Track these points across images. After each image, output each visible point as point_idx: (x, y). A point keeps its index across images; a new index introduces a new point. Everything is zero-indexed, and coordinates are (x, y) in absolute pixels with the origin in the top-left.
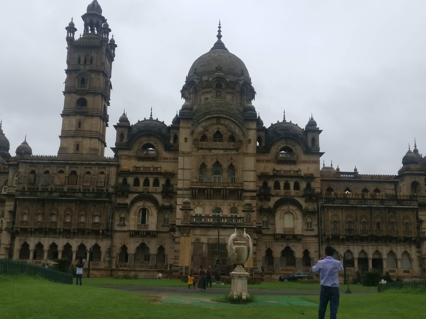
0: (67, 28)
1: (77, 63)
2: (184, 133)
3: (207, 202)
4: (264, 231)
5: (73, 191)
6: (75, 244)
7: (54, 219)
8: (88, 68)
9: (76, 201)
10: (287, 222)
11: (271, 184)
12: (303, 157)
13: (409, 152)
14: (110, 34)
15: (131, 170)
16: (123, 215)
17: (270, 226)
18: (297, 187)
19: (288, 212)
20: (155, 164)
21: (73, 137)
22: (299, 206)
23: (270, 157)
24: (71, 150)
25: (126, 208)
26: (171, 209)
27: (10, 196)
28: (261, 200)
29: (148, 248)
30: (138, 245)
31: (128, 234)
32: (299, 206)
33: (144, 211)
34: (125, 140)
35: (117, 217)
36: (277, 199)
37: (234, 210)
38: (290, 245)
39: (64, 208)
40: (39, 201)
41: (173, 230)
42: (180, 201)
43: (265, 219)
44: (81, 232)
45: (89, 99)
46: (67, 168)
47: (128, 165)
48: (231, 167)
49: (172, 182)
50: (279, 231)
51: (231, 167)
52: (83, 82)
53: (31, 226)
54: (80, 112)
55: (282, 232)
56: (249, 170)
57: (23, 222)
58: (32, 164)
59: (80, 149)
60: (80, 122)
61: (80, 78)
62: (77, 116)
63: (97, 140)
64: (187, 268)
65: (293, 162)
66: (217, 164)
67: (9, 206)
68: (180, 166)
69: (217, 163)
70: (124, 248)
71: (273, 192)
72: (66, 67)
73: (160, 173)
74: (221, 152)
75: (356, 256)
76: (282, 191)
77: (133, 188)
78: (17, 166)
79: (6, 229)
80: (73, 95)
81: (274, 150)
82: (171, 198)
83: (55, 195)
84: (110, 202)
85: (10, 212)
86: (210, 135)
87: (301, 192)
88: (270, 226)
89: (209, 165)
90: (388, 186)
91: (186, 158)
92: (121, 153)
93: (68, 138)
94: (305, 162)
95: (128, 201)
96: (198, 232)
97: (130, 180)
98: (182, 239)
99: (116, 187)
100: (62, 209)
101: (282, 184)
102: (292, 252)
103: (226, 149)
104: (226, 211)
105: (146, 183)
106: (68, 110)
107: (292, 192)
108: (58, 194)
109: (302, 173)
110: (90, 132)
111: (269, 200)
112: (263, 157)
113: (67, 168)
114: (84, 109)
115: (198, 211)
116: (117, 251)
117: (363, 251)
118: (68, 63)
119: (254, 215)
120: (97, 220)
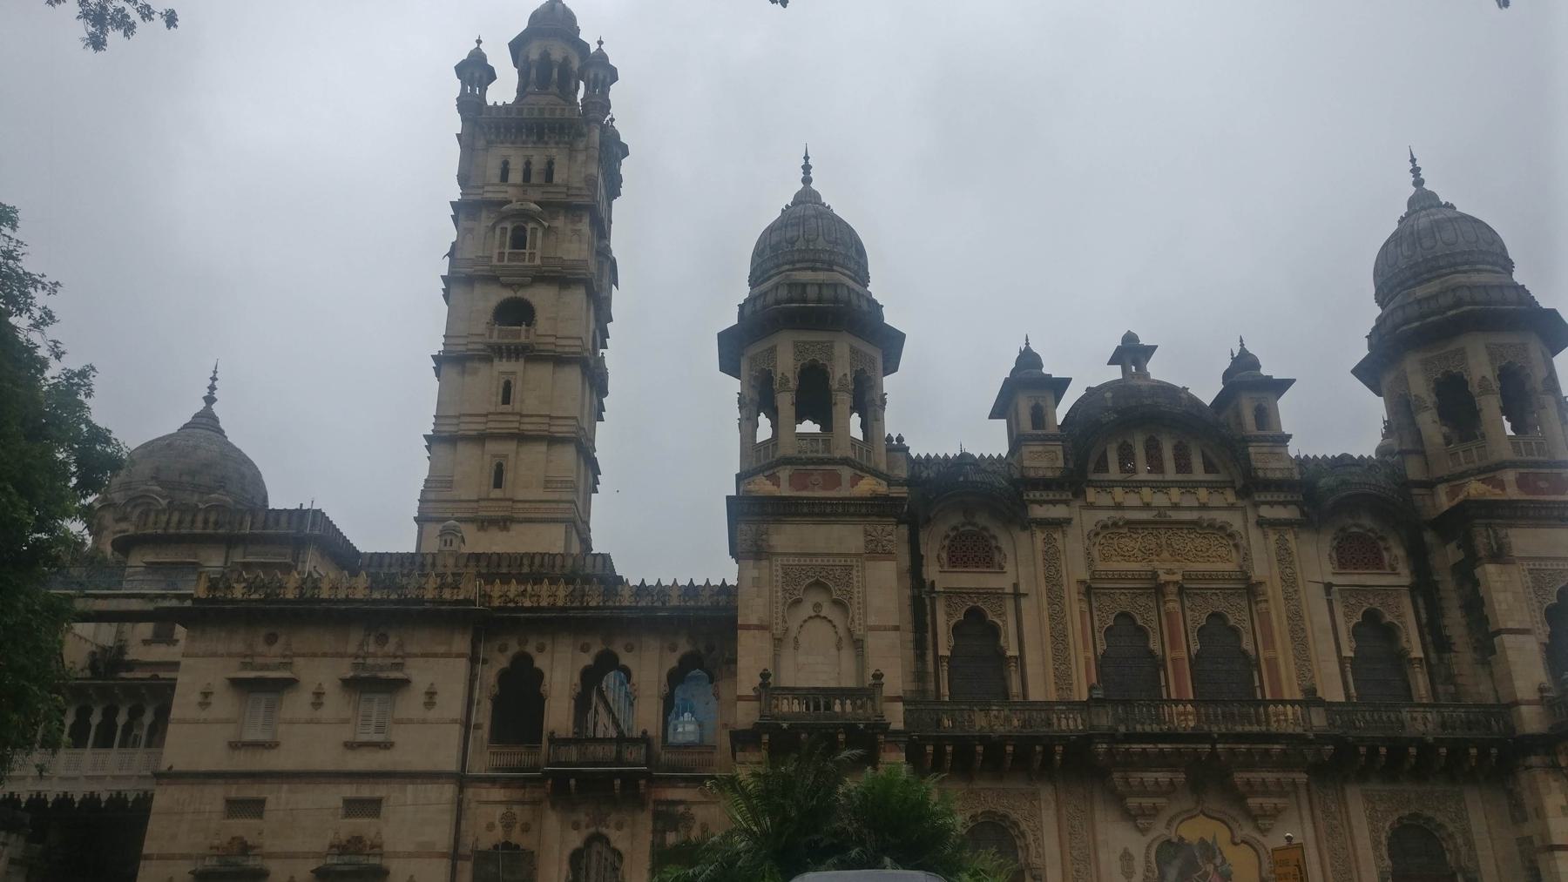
0: (461, 69)
1: (497, 180)
8: (537, 195)
45: (540, 297)
52: (519, 241)
54: (508, 347)
59: (508, 476)
60: (507, 388)
61: (509, 226)
62: (496, 361)
72: (457, 197)
80: (479, 290)
93: (461, 447)
106: (461, 341)
110: (547, 420)
114: (523, 334)
118: (463, 179)
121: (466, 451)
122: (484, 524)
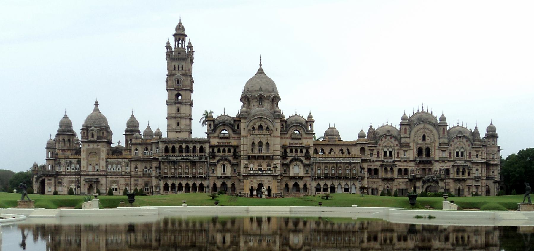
2: (242, 126)
3: (255, 162)
4: (284, 175)
5: (188, 156)
6: (191, 183)
7: (180, 171)
9: (190, 161)
10: (296, 170)
11: (288, 150)
12: (304, 136)
13: (362, 131)
14: (187, 40)
15: (217, 144)
16: (213, 168)
17: (287, 172)
18: (301, 151)
19: (296, 165)
20: (228, 141)
21: (175, 118)
22: (302, 162)
23: (288, 136)
24: (174, 125)
25: (214, 165)
26: (238, 165)
27: (156, 159)
28: (283, 159)
29: (226, 185)
30: (221, 183)
31: (216, 178)
32: (302, 162)
33: (224, 166)
34: (212, 128)
35: (210, 169)
36: (291, 158)
37: (269, 165)
38: (297, 181)
39: (185, 165)
40: (172, 162)
41: (239, 175)
42: (242, 161)
43: (285, 168)
44: (194, 177)
46: (184, 144)
47: (215, 141)
48: (267, 143)
49: (237, 150)
50: (292, 175)
51: (267, 143)
53: (169, 175)
55: (293, 175)
56: (276, 145)
57: (165, 173)
58: (165, 143)
63: (189, 119)
64: (247, 194)
65: (300, 139)
66: (260, 142)
67: (155, 164)
68: (242, 143)
69: (260, 141)
70: (215, 185)
71: (289, 154)
73: (231, 146)
74: (262, 136)
75: (329, 186)
76: (294, 154)
77: (217, 154)
78: (158, 143)
79: (155, 176)
81: (290, 132)
82: (237, 158)
83: (179, 158)
84: (207, 162)
85: (156, 167)
86: (256, 127)
87: (303, 154)
88: (287, 172)
89: (257, 143)
90: (353, 147)
91: (245, 139)
92: (210, 135)
94: (306, 138)
95: (215, 161)
96: (252, 178)
97: (216, 150)
98: (245, 181)
99: (209, 154)
100: (183, 165)
101: (294, 150)
102: (298, 185)
103: (264, 135)
104: (264, 166)
105: (224, 151)
107: (299, 154)
108: (180, 158)
109: (304, 145)
111: (287, 159)
112: (283, 136)
113: (184, 144)
115: (251, 166)
116: (211, 186)
117: (333, 184)
119: (279, 168)
120: (201, 171)
121: (173, 120)
122: (177, 132)
